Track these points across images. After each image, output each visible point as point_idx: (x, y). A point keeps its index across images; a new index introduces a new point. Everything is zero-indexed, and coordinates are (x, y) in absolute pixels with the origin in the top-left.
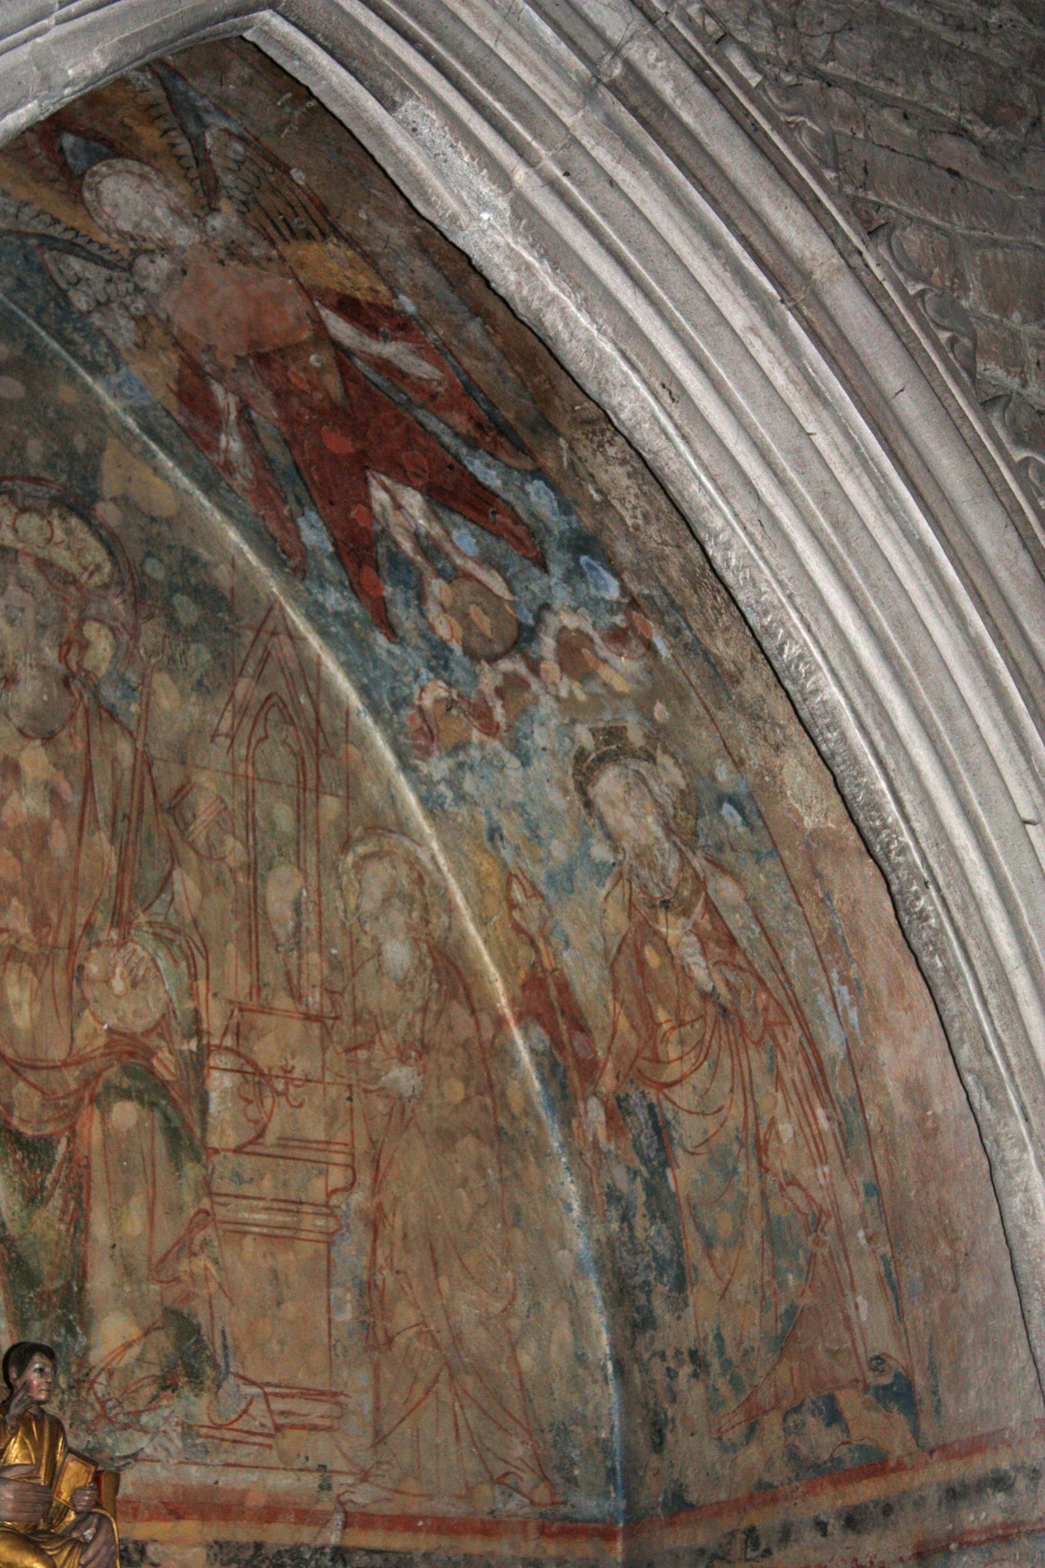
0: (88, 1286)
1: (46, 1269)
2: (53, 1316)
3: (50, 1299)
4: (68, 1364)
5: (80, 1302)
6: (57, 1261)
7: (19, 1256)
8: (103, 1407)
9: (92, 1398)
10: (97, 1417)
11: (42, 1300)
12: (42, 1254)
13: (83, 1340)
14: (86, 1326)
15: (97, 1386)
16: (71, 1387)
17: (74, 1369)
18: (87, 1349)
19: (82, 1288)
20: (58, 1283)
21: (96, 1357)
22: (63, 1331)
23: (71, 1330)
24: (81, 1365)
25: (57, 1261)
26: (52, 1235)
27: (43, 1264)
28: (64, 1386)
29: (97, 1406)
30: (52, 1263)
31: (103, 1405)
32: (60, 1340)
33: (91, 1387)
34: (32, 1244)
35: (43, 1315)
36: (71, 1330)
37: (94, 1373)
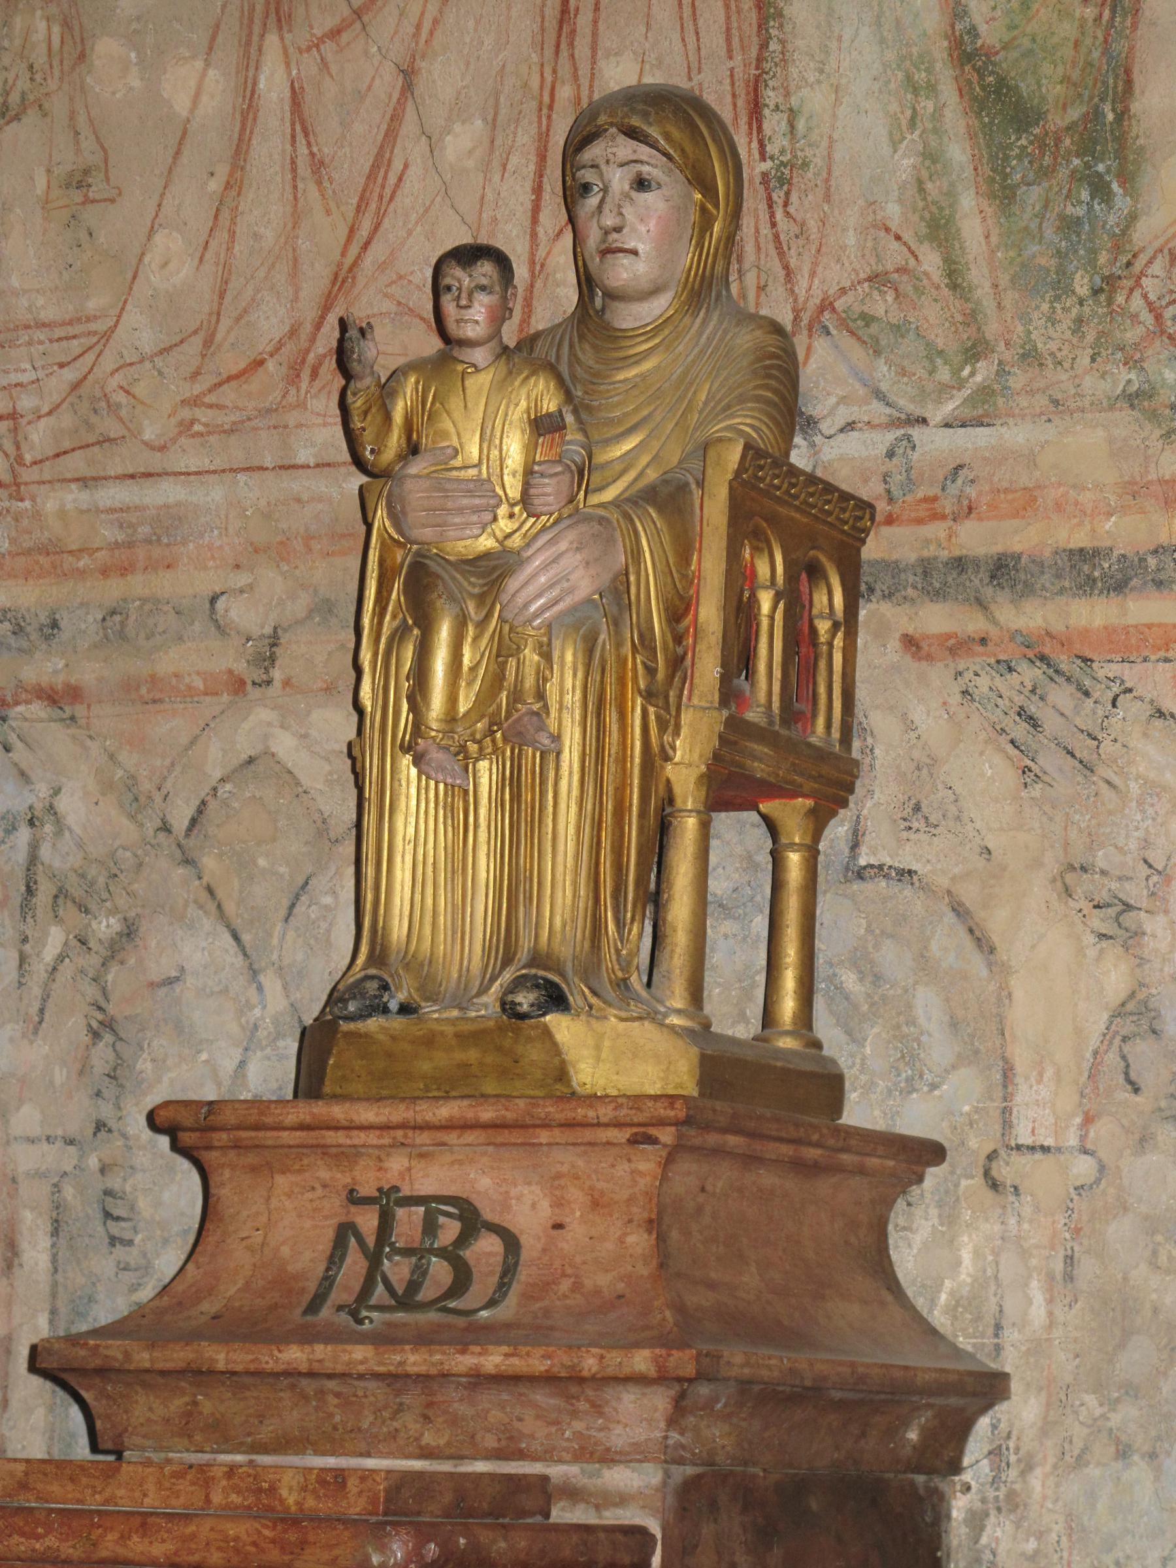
0: (1135, 107)
1: (1055, 91)
2: (1063, 173)
3: (1058, 141)
4: (1093, 252)
5: (1121, 140)
6: (1075, 75)
7: (1002, 81)
8: (1158, 318)
9: (1137, 303)
10: (1150, 336)
11: (1043, 147)
12: (1047, 68)
13: (1122, 202)
14: (1127, 178)
15: (1145, 281)
16: (1096, 292)
17: (1103, 258)
18: (1133, 217)
19: (1122, 115)
20: (1074, 114)
21: (1144, 233)
22: (1085, 195)
23: (1100, 190)
24: (1117, 249)
25: (1075, 75)
26: (1068, 29)
27: (1048, 86)
28: (1083, 290)
29: (1147, 318)
30: (1066, 79)
31: (1158, 318)
32: (1080, 211)
33: (1138, 284)
34: (1030, 53)
35: (1046, 173)
36: (1100, 190)
37: (1142, 260)
